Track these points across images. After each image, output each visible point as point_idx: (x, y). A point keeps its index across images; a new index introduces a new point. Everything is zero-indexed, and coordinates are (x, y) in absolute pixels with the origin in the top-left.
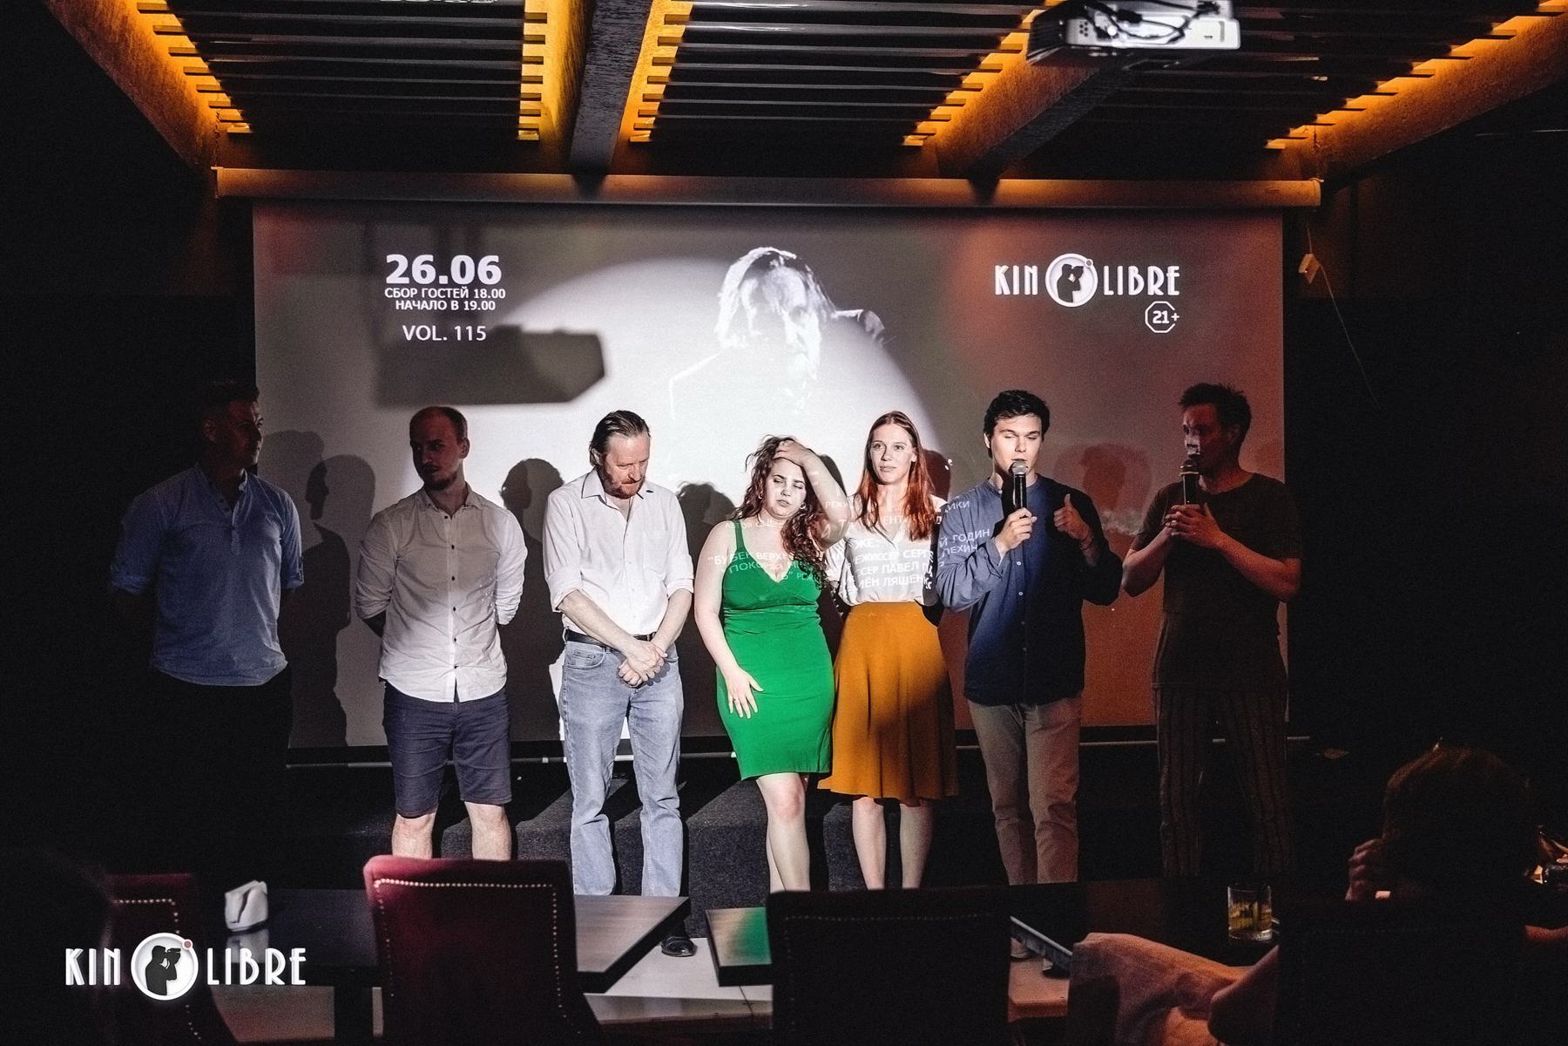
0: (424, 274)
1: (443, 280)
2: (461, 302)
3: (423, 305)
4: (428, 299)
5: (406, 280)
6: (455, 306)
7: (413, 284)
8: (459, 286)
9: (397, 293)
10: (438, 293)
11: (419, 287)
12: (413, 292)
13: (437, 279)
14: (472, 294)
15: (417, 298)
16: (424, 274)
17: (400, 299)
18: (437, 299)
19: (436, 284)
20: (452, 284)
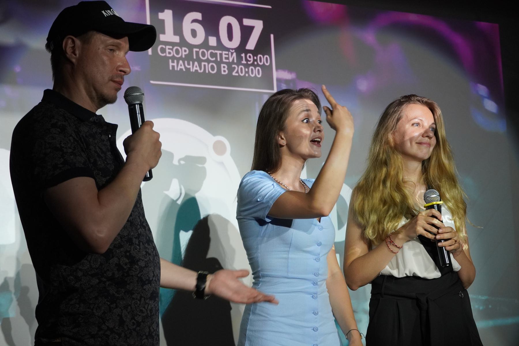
0: (194, 33)
1: (213, 41)
2: (229, 64)
3: (195, 67)
4: (200, 61)
5: (176, 39)
6: (224, 70)
7: (183, 43)
8: (228, 49)
9: (169, 52)
10: (208, 54)
11: (191, 47)
12: (184, 52)
13: (206, 40)
14: (239, 58)
15: (189, 58)
16: (194, 33)
17: (173, 58)
18: (208, 61)
19: (205, 45)
20: (220, 46)
